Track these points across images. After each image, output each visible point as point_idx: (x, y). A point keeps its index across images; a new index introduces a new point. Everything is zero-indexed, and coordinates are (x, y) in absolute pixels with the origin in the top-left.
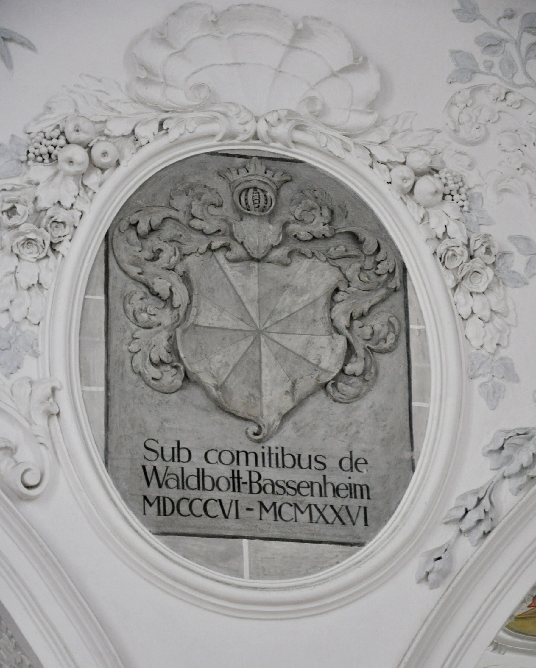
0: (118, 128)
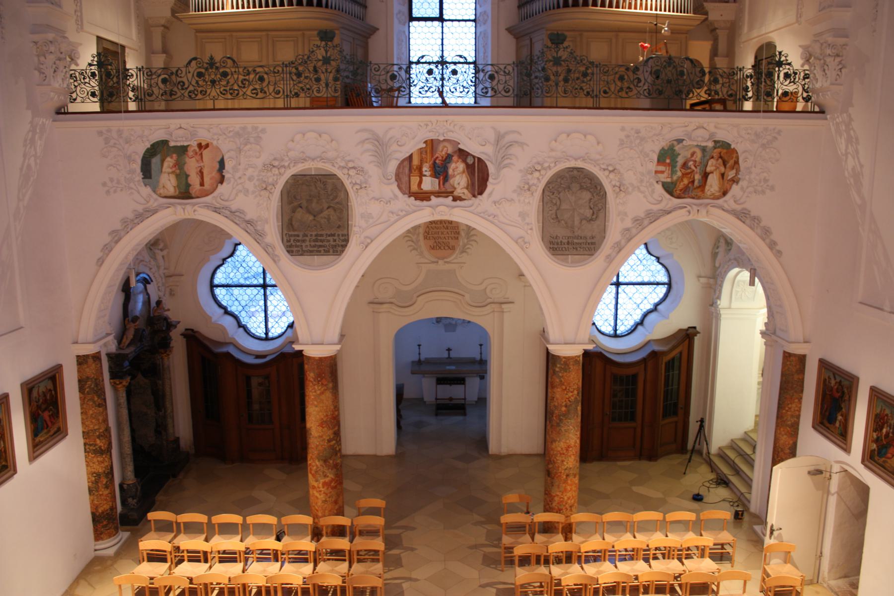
0: (546, 165)
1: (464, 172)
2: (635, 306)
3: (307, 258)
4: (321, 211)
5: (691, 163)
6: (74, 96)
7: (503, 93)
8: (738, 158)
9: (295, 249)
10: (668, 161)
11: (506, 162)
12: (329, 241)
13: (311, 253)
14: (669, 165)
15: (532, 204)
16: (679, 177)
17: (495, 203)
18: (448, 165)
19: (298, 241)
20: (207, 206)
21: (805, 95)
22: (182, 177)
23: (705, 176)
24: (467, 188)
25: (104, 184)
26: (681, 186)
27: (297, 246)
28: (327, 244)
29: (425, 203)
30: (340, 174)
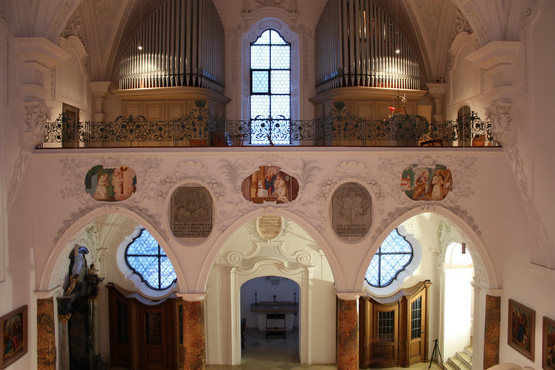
0: (334, 181)
1: (283, 186)
2: (391, 267)
3: (186, 239)
4: (195, 210)
5: (422, 179)
6: (47, 138)
7: (307, 137)
8: (451, 175)
9: (178, 233)
10: (408, 178)
11: (310, 179)
12: (200, 228)
13: (188, 235)
14: (409, 180)
15: (326, 205)
16: (415, 188)
17: (303, 204)
18: (274, 182)
19: (181, 228)
20: (125, 206)
21: (489, 136)
22: (110, 187)
23: (432, 186)
24: (285, 196)
25: (62, 192)
26: (417, 193)
27: (180, 231)
28: (199, 230)
29: (260, 205)
30: (207, 187)
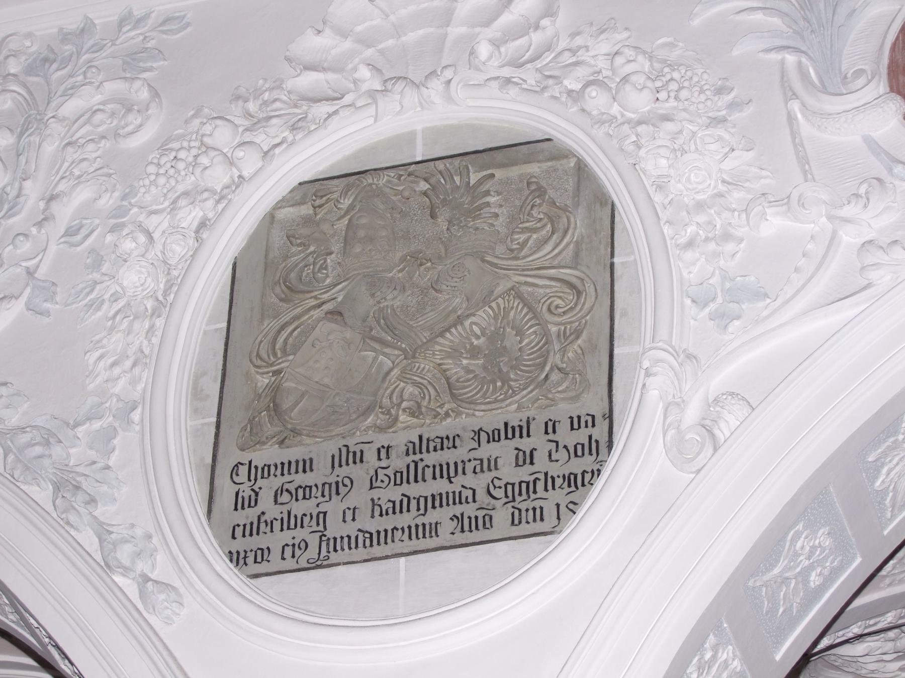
3: (350, 578)
9: (276, 540)
12: (493, 464)
13: (374, 543)
19: (306, 491)
27: (290, 522)
28: (480, 482)
